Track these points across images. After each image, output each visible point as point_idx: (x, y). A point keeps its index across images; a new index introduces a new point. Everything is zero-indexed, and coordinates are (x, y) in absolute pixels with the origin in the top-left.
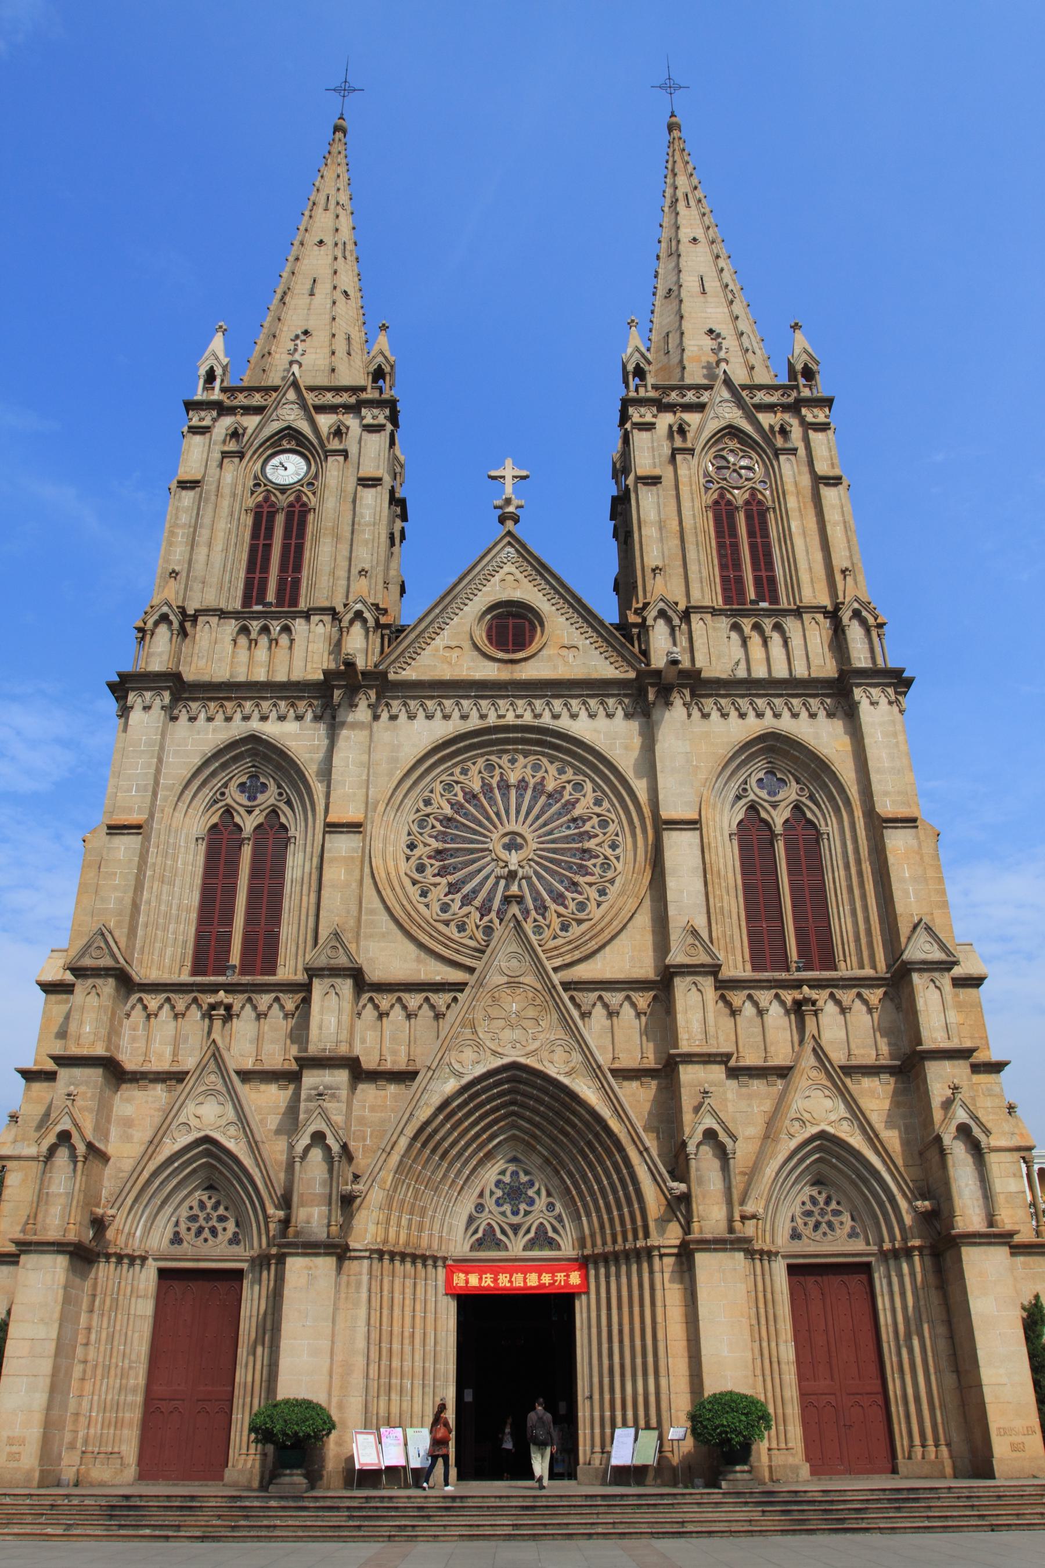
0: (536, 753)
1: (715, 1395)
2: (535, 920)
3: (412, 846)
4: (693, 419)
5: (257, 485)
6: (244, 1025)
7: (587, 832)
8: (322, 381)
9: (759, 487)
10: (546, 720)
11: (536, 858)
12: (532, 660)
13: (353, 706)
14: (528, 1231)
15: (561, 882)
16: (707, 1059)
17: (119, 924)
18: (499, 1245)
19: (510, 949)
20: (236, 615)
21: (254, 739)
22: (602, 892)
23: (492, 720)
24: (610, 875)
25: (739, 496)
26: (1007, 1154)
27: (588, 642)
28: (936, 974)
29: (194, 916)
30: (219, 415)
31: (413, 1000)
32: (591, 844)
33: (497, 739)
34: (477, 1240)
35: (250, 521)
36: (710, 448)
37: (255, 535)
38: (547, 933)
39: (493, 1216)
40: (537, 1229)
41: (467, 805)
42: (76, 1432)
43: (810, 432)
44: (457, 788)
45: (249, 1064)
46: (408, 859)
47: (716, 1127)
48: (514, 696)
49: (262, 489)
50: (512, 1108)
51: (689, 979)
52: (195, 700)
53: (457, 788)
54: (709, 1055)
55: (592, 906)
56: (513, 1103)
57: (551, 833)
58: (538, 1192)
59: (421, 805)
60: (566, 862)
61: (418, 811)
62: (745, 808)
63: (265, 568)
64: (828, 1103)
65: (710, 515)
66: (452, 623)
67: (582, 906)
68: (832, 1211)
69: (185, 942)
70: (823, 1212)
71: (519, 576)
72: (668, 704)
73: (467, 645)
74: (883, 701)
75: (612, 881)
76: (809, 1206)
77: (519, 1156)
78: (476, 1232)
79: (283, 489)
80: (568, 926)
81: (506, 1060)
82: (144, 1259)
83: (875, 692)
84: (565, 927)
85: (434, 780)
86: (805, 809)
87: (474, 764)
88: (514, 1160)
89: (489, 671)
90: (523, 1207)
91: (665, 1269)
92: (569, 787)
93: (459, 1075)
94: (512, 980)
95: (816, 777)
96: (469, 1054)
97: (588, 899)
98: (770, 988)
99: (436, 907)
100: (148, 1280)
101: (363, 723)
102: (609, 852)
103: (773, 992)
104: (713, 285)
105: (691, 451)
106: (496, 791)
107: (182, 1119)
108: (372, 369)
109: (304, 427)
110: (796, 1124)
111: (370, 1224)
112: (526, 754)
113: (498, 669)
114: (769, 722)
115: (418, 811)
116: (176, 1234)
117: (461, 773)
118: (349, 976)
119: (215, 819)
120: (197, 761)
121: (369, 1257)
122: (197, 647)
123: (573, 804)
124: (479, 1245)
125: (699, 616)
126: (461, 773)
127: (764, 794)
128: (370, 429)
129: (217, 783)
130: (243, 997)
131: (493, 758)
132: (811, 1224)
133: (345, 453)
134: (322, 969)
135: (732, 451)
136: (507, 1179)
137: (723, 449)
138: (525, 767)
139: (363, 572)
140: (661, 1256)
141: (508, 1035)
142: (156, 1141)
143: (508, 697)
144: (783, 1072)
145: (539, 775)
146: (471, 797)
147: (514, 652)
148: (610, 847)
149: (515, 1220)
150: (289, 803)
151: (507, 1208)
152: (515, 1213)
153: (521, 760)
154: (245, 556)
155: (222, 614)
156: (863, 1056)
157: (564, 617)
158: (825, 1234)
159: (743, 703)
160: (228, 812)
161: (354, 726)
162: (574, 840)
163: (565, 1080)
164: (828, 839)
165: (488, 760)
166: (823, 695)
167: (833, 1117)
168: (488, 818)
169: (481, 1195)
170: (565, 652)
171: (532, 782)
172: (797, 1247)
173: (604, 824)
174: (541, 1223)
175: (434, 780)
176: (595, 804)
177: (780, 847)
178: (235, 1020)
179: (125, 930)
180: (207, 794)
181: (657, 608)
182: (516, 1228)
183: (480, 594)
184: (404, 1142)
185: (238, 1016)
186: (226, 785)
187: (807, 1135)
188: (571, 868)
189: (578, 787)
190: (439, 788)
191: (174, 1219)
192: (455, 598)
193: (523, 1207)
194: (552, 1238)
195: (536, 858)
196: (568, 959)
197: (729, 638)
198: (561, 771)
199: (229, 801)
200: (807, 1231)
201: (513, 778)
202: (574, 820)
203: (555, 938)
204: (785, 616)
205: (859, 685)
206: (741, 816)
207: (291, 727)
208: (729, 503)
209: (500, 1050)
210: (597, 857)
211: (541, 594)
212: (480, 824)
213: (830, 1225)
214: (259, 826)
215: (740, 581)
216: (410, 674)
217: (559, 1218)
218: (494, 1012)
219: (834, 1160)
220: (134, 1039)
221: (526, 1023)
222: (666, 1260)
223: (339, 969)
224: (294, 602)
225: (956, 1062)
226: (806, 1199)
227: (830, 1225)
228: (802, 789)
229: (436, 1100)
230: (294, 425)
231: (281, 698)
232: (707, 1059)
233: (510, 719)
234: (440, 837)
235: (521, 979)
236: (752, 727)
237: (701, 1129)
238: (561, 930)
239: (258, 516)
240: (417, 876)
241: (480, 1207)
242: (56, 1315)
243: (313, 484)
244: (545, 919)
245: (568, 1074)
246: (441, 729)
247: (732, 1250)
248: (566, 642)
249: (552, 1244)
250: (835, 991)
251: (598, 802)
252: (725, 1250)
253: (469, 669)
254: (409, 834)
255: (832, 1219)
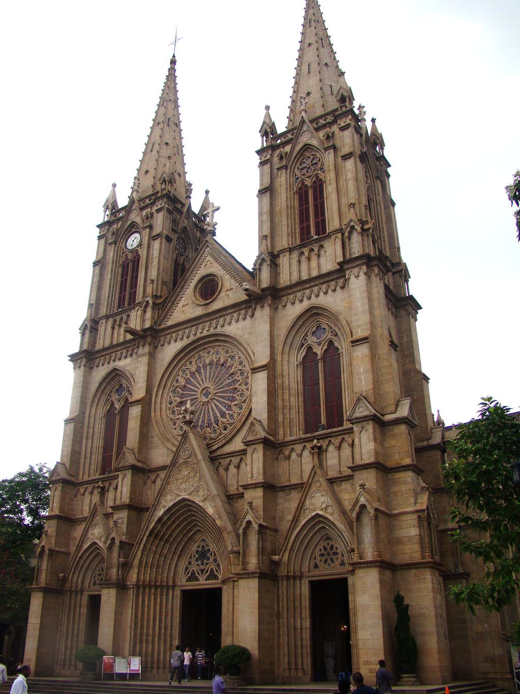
0: (217, 346)
1: (226, 646)
2: (214, 428)
3: (171, 403)
4: (288, 148)
5: (123, 253)
6: (111, 495)
7: (236, 379)
8: (150, 192)
9: (320, 172)
10: (219, 330)
11: (216, 398)
12: (215, 301)
13: (144, 346)
14: (207, 572)
15: (225, 407)
16: (255, 486)
17: (67, 460)
18: (197, 579)
19: (185, 447)
20: (114, 315)
21: (115, 370)
22: (241, 408)
23: (199, 335)
24: (244, 399)
25: (308, 182)
26: (411, 515)
27: (238, 284)
28: (365, 423)
29: (101, 450)
30: (110, 226)
31: (162, 474)
32: (237, 386)
33: (201, 344)
34: (189, 577)
35: (120, 271)
36: (298, 160)
37: (122, 277)
38: (218, 431)
39: (194, 568)
40: (210, 571)
41: (191, 379)
42: (58, 658)
43: (341, 132)
44: (187, 371)
45: (110, 510)
46: (169, 409)
47: (251, 519)
48: (205, 322)
49: (124, 254)
50: (192, 518)
51: (253, 447)
52: (97, 358)
53: (187, 371)
54: (255, 484)
55: (235, 415)
56: (194, 516)
57: (222, 383)
58: (211, 554)
59: (175, 382)
60: (227, 396)
61: (174, 386)
62: (305, 350)
63: (125, 291)
64: (323, 499)
65: (296, 197)
66: (186, 293)
67: (232, 416)
68: (333, 553)
69: (98, 461)
70: (329, 555)
71: (212, 260)
72: (262, 307)
73: (190, 302)
74: (362, 274)
75: (244, 402)
76: (323, 551)
77: (205, 538)
78: (188, 573)
79: (131, 251)
80: (227, 427)
81: (181, 497)
82: (82, 592)
83: (356, 270)
84: (225, 429)
85: (179, 370)
86: (334, 341)
87: (194, 358)
88: (203, 540)
89: (199, 311)
90: (205, 561)
91: (235, 587)
92: (229, 359)
93: (165, 507)
94: (185, 460)
95: (336, 325)
96: (169, 497)
97: (234, 413)
98: (301, 443)
99: (178, 430)
100: (85, 600)
101: (146, 353)
102: (244, 387)
103: (303, 444)
104: (314, 67)
105: (286, 167)
106: (202, 369)
107: (88, 536)
108: (161, 182)
109: (138, 220)
110: (308, 511)
111: (134, 575)
112: (214, 347)
113: (202, 310)
114: (314, 301)
115: (174, 386)
116: (95, 581)
117: (190, 364)
118: (130, 469)
119: (108, 407)
120: (97, 385)
121: (133, 588)
122: (99, 335)
123: (231, 367)
124: (189, 580)
125: (283, 254)
126: (190, 364)
127: (315, 340)
128: (158, 211)
129: (107, 391)
130: (108, 482)
131: (201, 353)
132: (323, 561)
133: (151, 227)
134: (121, 468)
135: (309, 157)
136: (200, 549)
137: (303, 159)
138: (213, 354)
139: (153, 281)
140: (234, 581)
141: (183, 486)
142: (79, 546)
143: (203, 323)
144: (300, 486)
145: (218, 356)
146: (192, 374)
147: (210, 298)
148: (245, 384)
149: (202, 567)
150: (131, 394)
151: (200, 562)
152: (202, 564)
153: (211, 350)
154: (118, 287)
155: (107, 317)
156: (345, 471)
157: (229, 275)
158: (329, 565)
159: (299, 294)
160: (113, 404)
161: (143, 355)
162: (231, 385)
163: (201, 504)
164: (343, 356)
165: (199, 355)
166: (337, 278)
167: (324, 506)
168: (198, 383)
169: (191, 558)
170: (228, 293)
171: (215, 360)
172: (317, 572)
173: (242, 373)
174: (212, 568)
175: (179, 370)
176: (239, 365)
177: (320, 365)
178: (106, 493)
179: (69, 463)
180: (104, 398)
181: (261, 258)
182: (202, 571)
183: (197, 275)
184: (145, 538)
185: (108, 490)
186: (111, 392)
187: (310, 517)
188: (229, 399)
189: (232, 357)
190: (181, 373)
191: (94, 575)
192: (186, 281)
193: (205, 561)
194: (216, 575)
195: (216, 398)
196: (220, 444)
197: (299, 262)
198: (227, 352)
199: (113, 398)
200: (321, 565)
201: (208, 362)
202: (232, 374)
203: (222, 434)
204: (324, 240)
205: (348, 269)
206: (304, 354)
207: (128, 360)
208: (306, 186)
209: (179, 494)
210: (239, 391)
211: (220, 267)
212: (195, 386)
213: (332, 561)
214: (123, 407)
215: (309, 227)
216: (169, 323)
217: (218, 565)
218: (179, 476)
219: (328, 528)
220: (78, 505)
221: (191, 479)
222: (235, 583)
223: (126, 467)
224: (134, 301)
225: (369, 470)
226: (322, 547)
227: (332, 561)
228: (332, 332)
229: (156, 519)
230: (134, 220)
231: (123, 349)
232: (255, 486)
233: (205, 333)
234: (182, 396)
235: (188, 460)
236: (306, 304)
237: (246, 520)
238: (224, 430)
239: (124, 266)
240: (172, 416)
241: (190, 563)
242: (40, 615)
243: (141, 245)
244: (218, 426)
245: (203, 501)
246: (179, 345)
247: (253, 577)
248: (229, 288)
249: (216, 578)
250: (331, 439)
251: (241, 363)
252: (250, 578)
253: (191, 313)
254: (170, 398)
255: (333, 557)
